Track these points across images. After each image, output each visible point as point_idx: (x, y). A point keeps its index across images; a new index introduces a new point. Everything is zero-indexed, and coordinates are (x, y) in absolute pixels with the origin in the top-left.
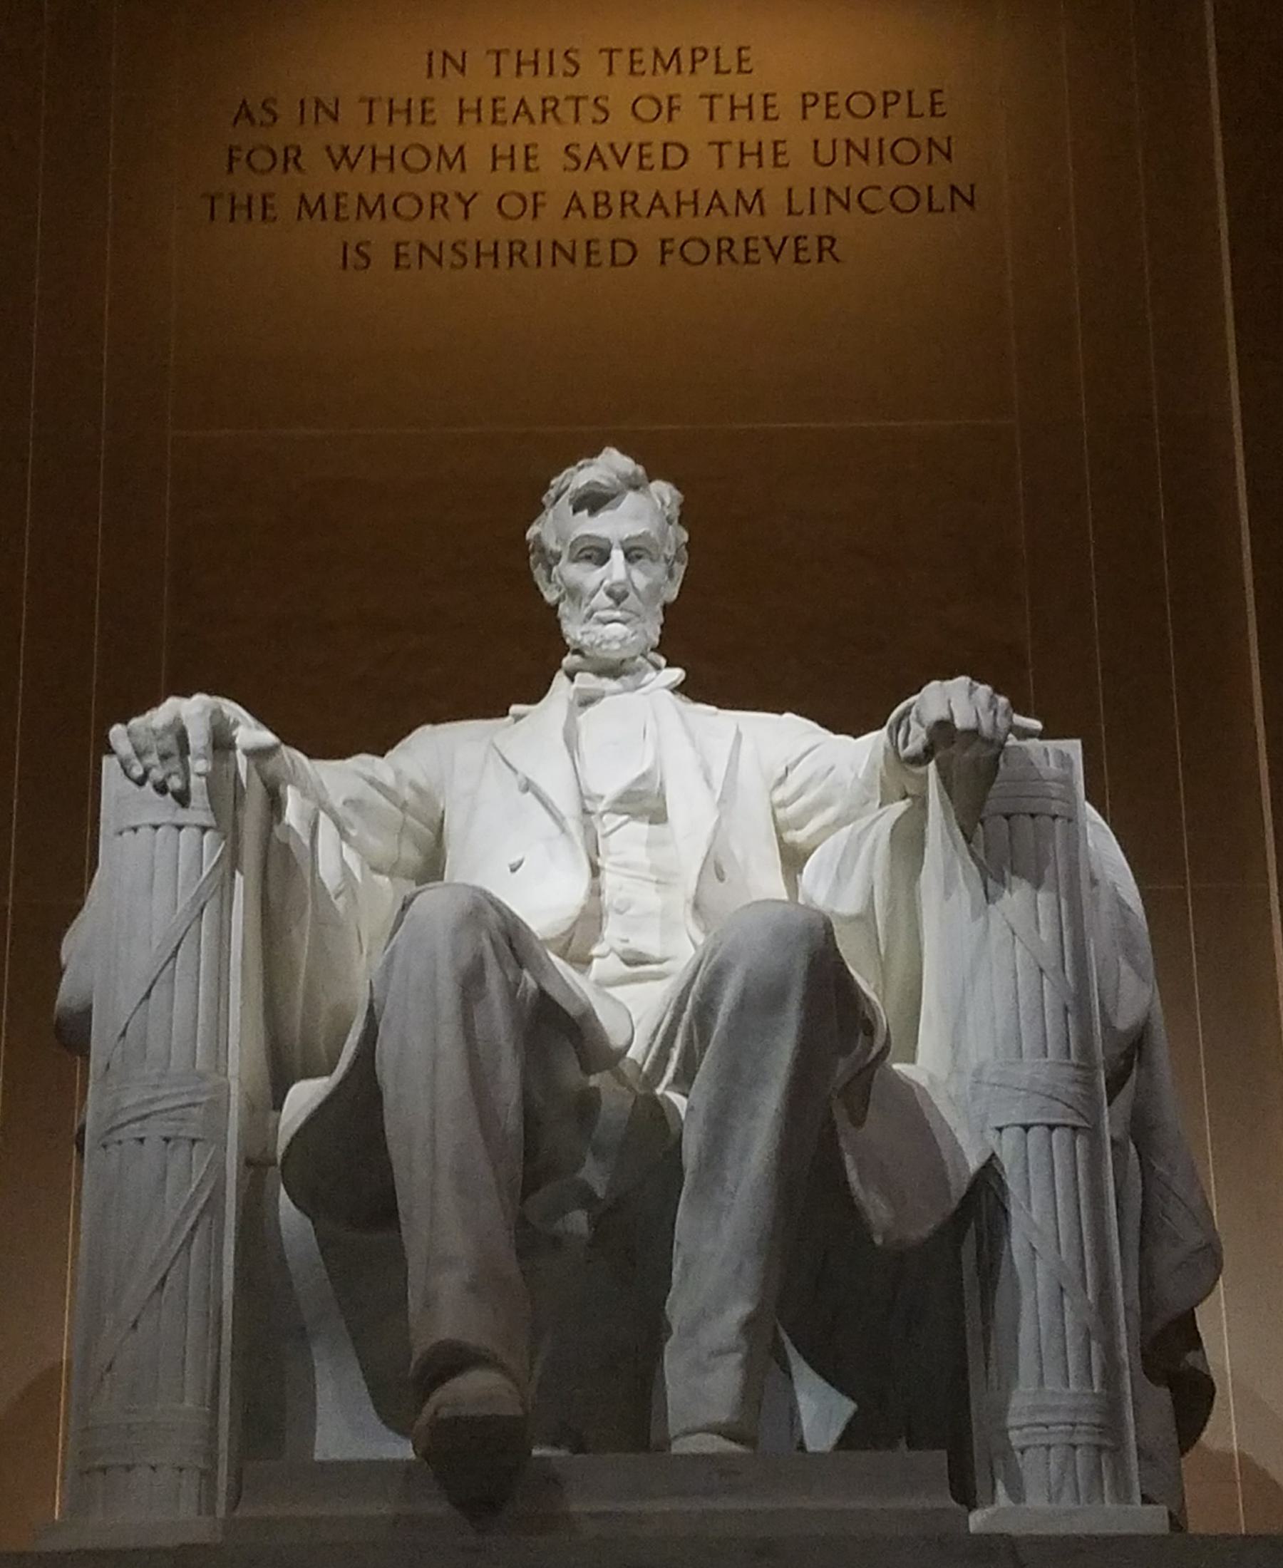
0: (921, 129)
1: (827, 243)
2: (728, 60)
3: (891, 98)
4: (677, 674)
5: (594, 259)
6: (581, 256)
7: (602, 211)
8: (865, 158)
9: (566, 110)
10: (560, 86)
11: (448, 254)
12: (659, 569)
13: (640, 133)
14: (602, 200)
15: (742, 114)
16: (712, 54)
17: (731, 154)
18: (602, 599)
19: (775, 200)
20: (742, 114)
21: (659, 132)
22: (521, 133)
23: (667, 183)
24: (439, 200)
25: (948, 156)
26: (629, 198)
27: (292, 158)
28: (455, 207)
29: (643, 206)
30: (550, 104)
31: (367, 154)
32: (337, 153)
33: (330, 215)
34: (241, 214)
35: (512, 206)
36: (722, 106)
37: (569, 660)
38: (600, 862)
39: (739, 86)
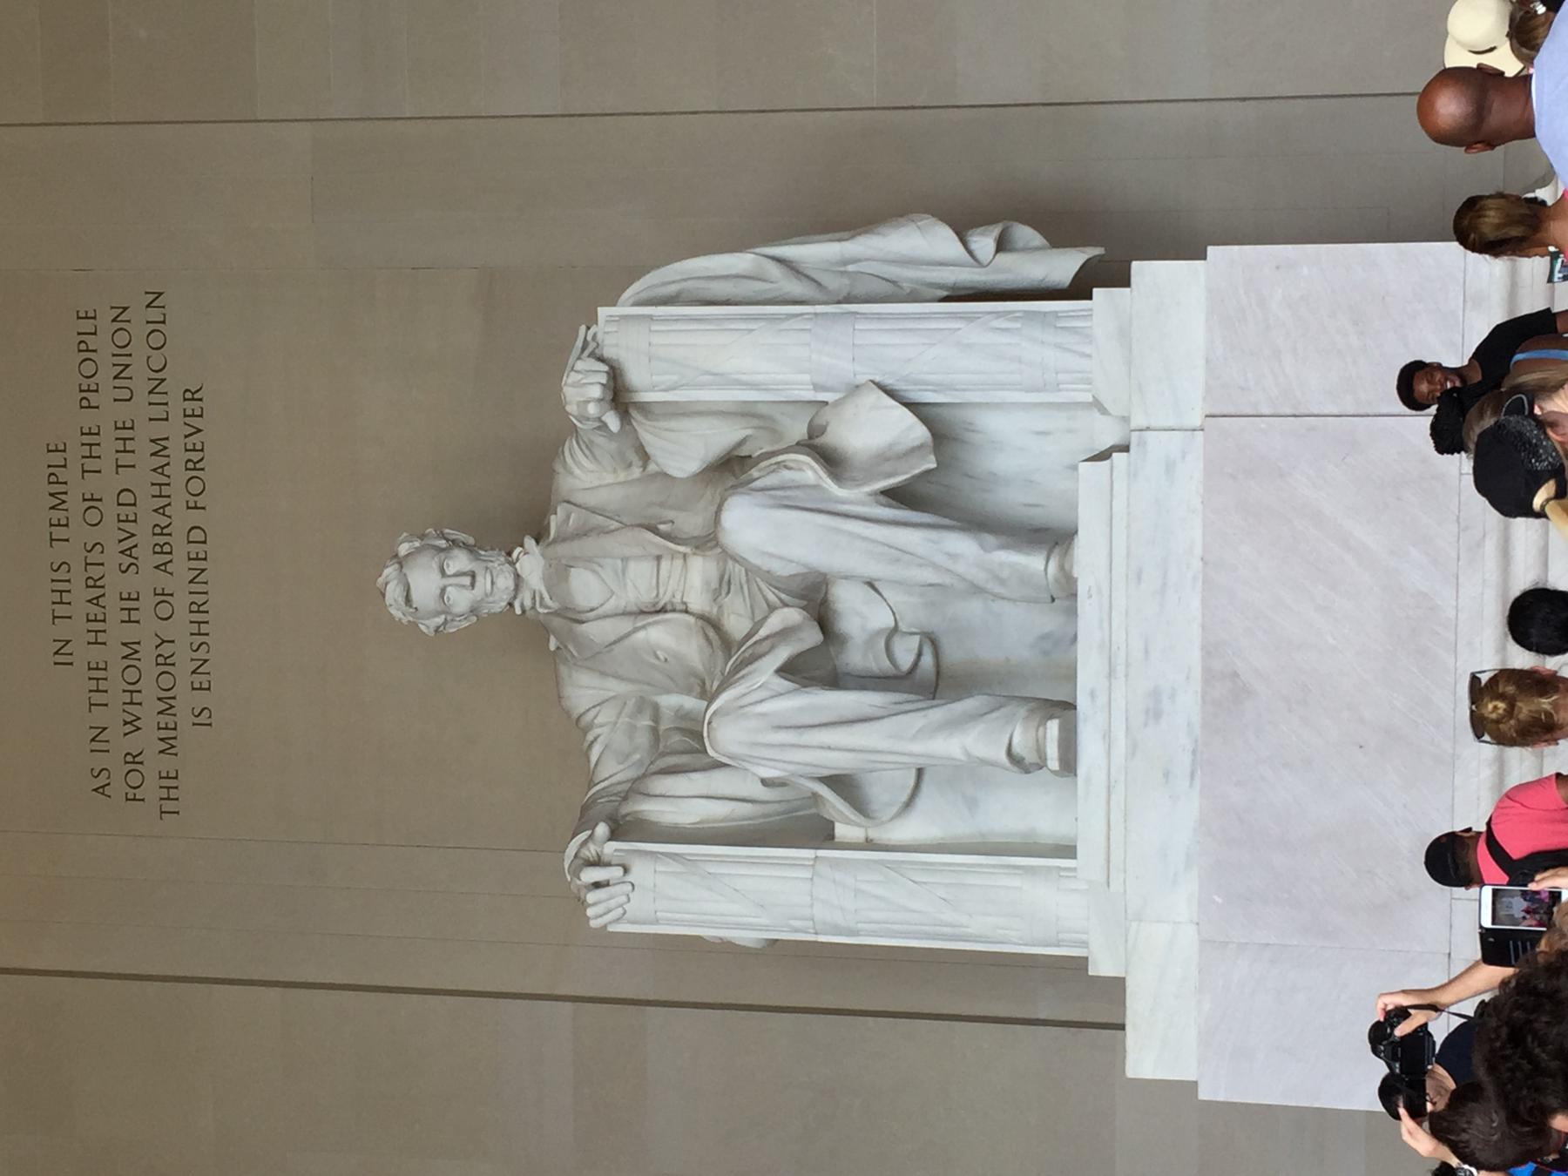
0: (105, 324)
1: (188, 395)
2: (57, 459)
3: (83, 346)
4: (529, 542)
5: (202, 555)
6: (201, 564)
7: (167, 548)
8: (127, 366)
9: (95, 572)
10: (78, 576)
11: (201, 654)
12: (456, 552)
13: (110, 520)
14: (159, 550)
15: (96, 451)
16: (52, 470)
17: (125, 459)
18: (478, 592)
19: (158, 430)
20: (96, 451)
21: (110, 509)
22: (111, 602)
23: (146, 504)
24: (161, 660)
25: (125, 309)
26: (158, 530)
27: (134, 759)
28: (166, 650)
29: (164, 521)
30: (91, 582)
31: (129, 708)
32: (129, 728)
33: (172, 734)
34: (173, 794)
35: (164, 610)
36: (91, 464)
37: (518, 611)
38: (661, 604)
39: (75, 453)
